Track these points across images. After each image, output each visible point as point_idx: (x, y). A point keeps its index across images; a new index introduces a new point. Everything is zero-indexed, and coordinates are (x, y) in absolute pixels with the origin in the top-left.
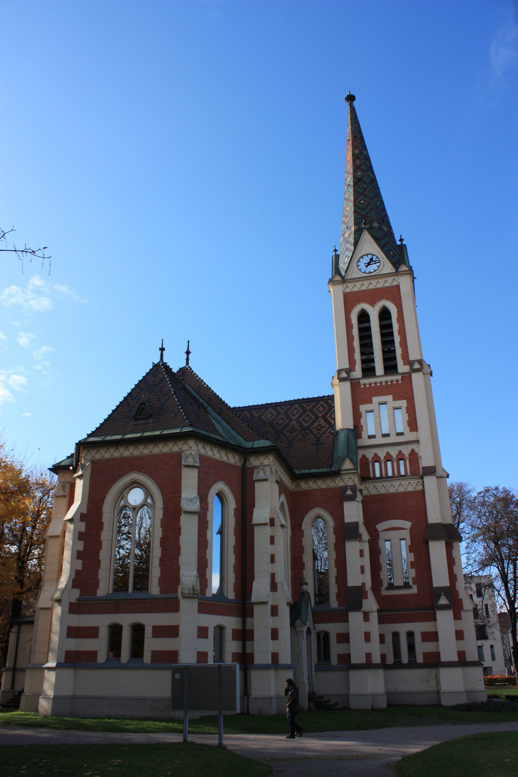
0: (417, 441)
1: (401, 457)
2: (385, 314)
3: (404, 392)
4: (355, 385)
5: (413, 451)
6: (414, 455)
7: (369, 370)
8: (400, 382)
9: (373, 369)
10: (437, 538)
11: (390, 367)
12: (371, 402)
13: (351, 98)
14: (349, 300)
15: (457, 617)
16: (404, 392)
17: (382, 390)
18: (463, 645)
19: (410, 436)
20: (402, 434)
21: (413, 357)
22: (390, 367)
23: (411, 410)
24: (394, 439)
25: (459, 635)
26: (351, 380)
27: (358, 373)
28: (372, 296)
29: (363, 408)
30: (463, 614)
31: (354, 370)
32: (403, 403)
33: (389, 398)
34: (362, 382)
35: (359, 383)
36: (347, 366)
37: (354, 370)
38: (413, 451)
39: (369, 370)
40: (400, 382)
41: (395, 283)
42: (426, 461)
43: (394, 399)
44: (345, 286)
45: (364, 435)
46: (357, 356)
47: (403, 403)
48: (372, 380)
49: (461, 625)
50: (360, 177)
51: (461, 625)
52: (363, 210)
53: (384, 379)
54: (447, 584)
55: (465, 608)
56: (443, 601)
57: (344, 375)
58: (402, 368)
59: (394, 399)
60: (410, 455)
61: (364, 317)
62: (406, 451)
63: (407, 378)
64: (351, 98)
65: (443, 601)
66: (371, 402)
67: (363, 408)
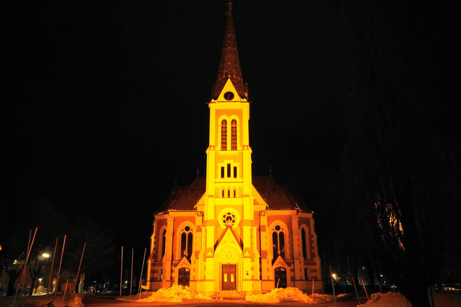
2: (234, 122)
15: (253, 260)
25: (252, 269)
56: (247, 254)
61: (224, 122)
65: (247, 254)
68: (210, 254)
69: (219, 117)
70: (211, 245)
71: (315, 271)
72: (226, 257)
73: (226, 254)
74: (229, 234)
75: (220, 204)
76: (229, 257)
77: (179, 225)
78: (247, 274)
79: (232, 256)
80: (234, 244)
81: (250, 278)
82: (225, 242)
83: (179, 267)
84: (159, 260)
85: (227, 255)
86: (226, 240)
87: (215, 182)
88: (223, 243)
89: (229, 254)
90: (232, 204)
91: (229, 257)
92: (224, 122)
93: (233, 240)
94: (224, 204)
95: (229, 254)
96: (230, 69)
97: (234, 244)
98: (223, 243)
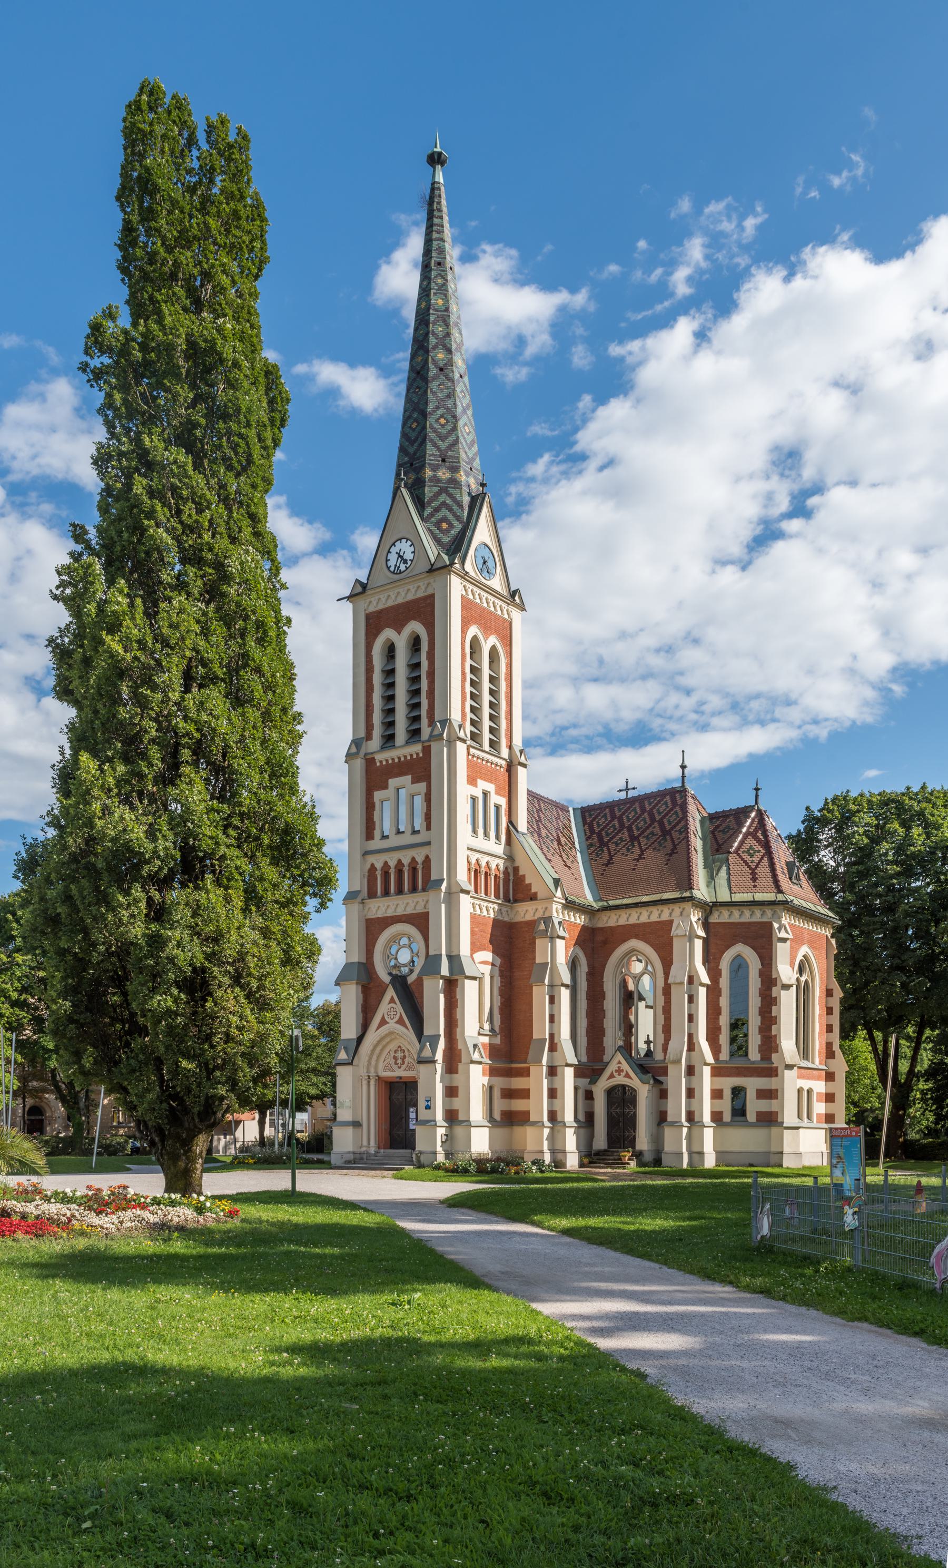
0: (429, 843)
7: (389, 739)
12: (386, 787)
22: (414, 734)
24: (408, 839)
32: (422, 786)
35: (374, 759)
39: (389, 739)
43: (413, 783)
59: (413, 783)
60: (424, 862)
66: (386, 787)
67: (378, 795)
73: (392, 1054)
75: (380, 914)
76: (399, 1061)
79: (406, 1061)
82: (383, 1022)
85: (395, 1058)
89: (399, 1055)
90: (410, 911)
91: (399, 1061)
93: (401, 1019)
95: (399, 1055)
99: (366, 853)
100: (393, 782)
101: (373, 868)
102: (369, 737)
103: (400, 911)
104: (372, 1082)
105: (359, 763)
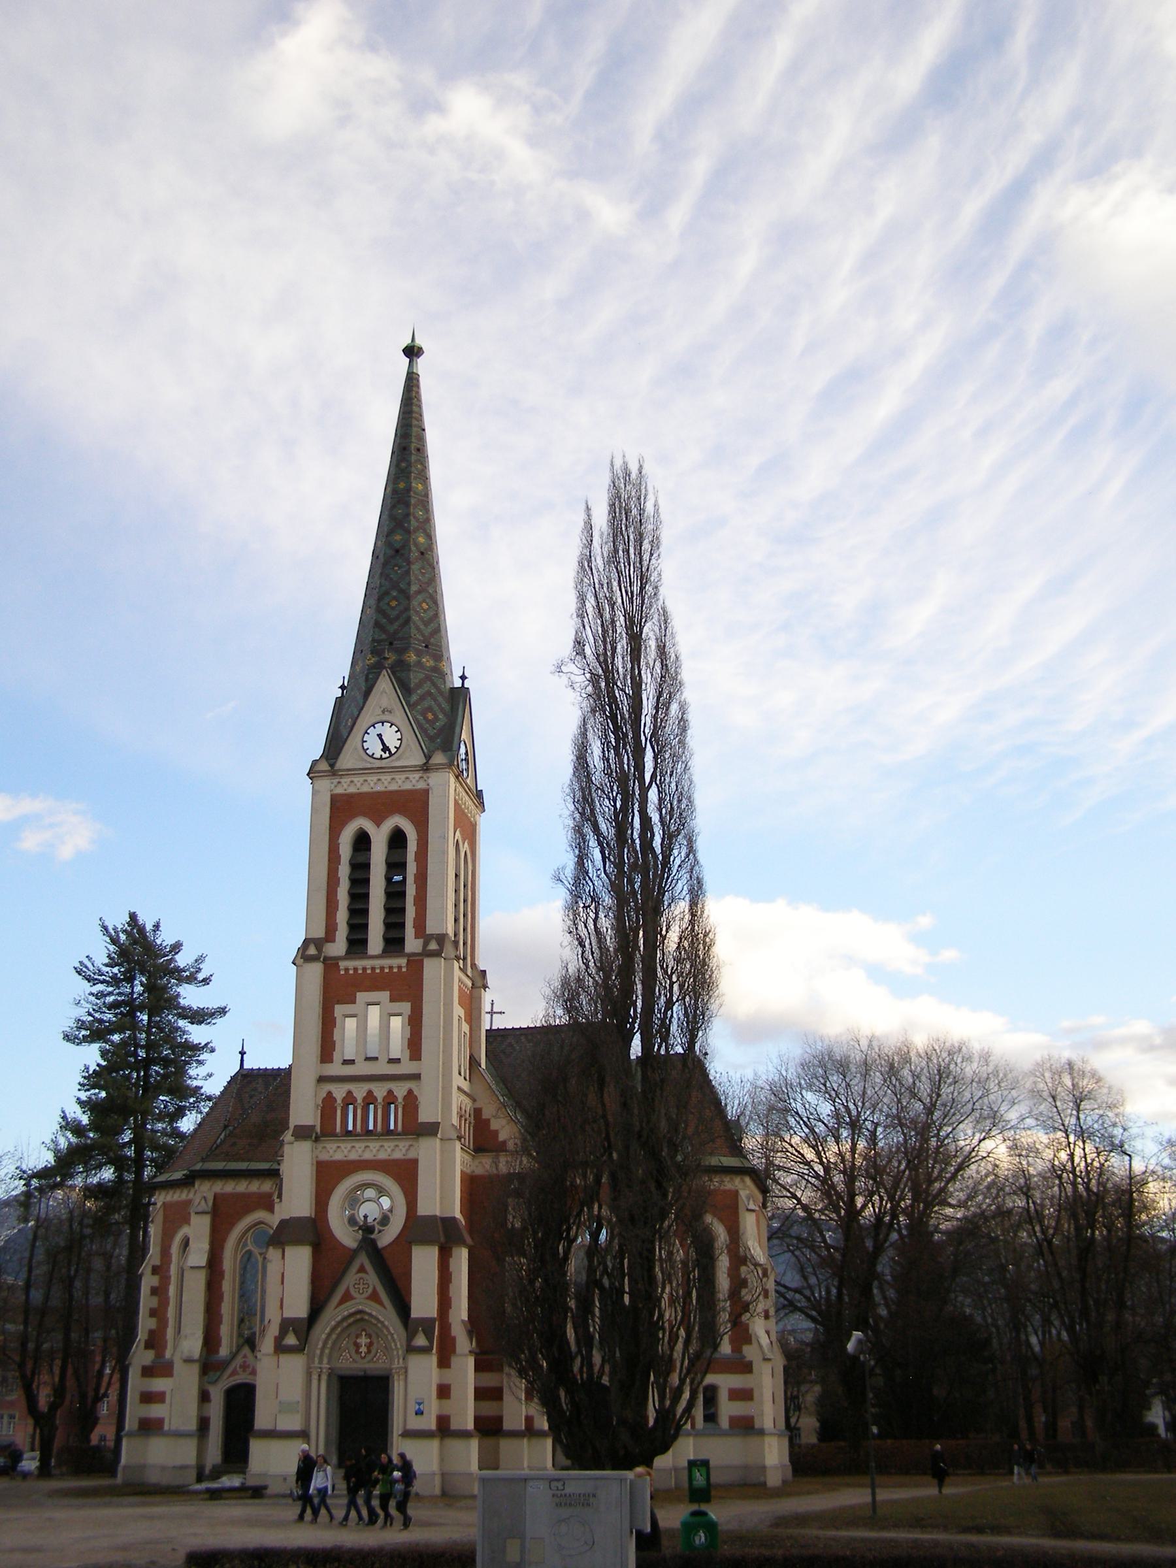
0: (417, 1077)
1: (390, 1098)
2: (397, 840)
3: (407, 989)
4: (330, 965)
5: (410, 1092)
6: (411, 1102)
7: (357, 943)
8: (404, 970)
9: (364, 942)
10: (425, 1241)
11: (393, 943)
13: (412, 352)
14: (341, 809)
15: (444, 1362)
16: (407, 989)
17: (374, 982)
18: (449, 1407)
19: (407, 1067)
20: (398, 1061)
21: (431, 929)
22: (393, 943)
23: (415, 1022)
24: (382, 1068)
25: (444, 1392)
26: (326, 959)
27: (339, 947)
28: (379, 805)
29: (339, 1010)
30: (454, 1360)
31: (333, 941)
32: (406, 1007)
33: (384, 996)
34: (343, 964)
36: (320, 933)
37: (333, 941)
38: (410, 1092)
39: (357, 943)
40: (404, 970)
41: (421, 785)
42: (424, 1116)
43: (392, 1000)
44: (336, 781)
45: (337, 1056)
46: (342, 916)
47: (406, 1007)
48: (359, 964)
49: (449, 1376)
50: (397, 546)
51: (449, 1376)
52: (391, 622)
53: (378, 963)
54: (434, 1313)
55: (458, 1349)
56: (420, 1340)
57: (312, 951)
58: (412, 944)
59: (392, 1000)
60: (405, 1098)
61: (362, 842)
62: (400, 1090)
63: (416, 963)
64: (412, 352)
65: (420, 1340)
67: (339, 1010)
68: (291, 1340)
69: (344, 824)
70: (299, 1308)
71: (744, 1395)
72: (353, 1349)
74: (362, 1269)
75: (338, 1156)
76: (363, 1349)
77: (232, 1225)
78: (419, 1413)
79: (373, 1352)
80: (381, 1303)
81: (433, 1426)
83: (226, 1382)
84: (168, 1355)
86: (352, 1291)
87: (322, 1079)
88: (341, 1303)
90: (382, 1156)
91: (363, 1349)
92: (362, 842)
94: (353, 1156)
96: (396, 626)
97: (381, 1303)
98: (341, 1303)
99: (322, 1079)
100: (362, 997)
101: (329, 1098)
102: (330, 936)
103: (368, 1156)
104: (324, 1378)
105: (316, 970)
